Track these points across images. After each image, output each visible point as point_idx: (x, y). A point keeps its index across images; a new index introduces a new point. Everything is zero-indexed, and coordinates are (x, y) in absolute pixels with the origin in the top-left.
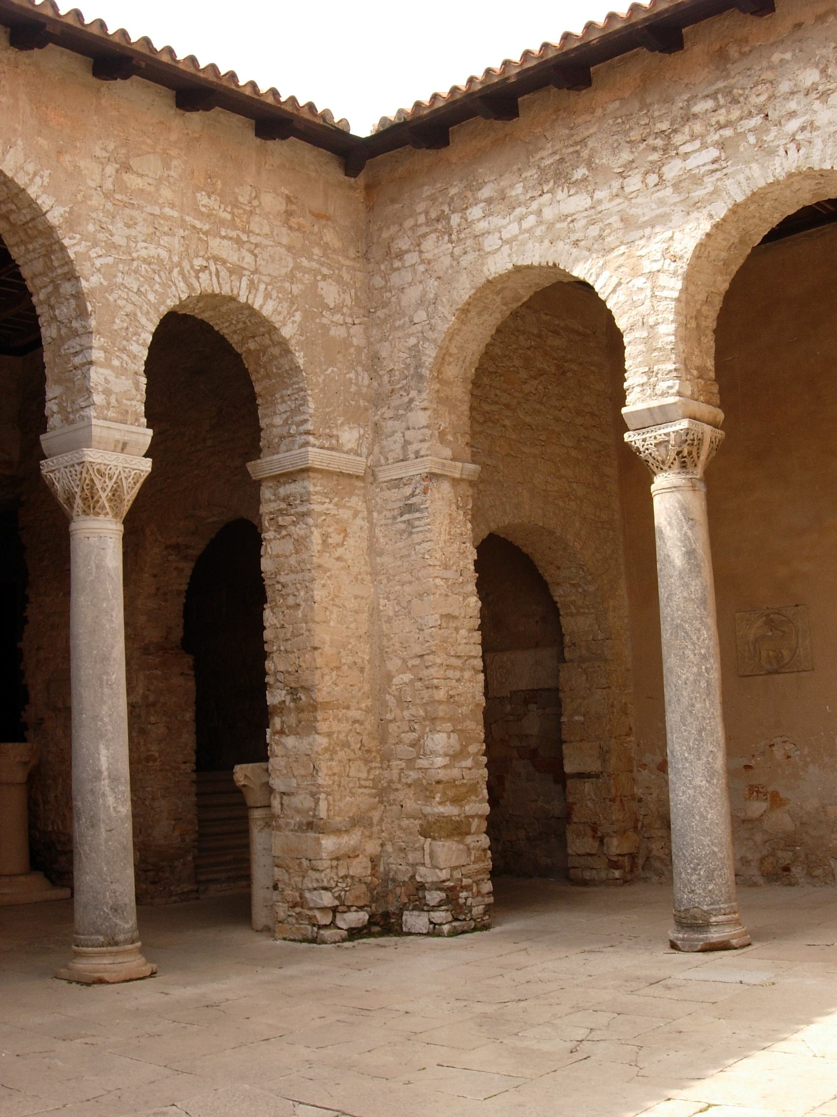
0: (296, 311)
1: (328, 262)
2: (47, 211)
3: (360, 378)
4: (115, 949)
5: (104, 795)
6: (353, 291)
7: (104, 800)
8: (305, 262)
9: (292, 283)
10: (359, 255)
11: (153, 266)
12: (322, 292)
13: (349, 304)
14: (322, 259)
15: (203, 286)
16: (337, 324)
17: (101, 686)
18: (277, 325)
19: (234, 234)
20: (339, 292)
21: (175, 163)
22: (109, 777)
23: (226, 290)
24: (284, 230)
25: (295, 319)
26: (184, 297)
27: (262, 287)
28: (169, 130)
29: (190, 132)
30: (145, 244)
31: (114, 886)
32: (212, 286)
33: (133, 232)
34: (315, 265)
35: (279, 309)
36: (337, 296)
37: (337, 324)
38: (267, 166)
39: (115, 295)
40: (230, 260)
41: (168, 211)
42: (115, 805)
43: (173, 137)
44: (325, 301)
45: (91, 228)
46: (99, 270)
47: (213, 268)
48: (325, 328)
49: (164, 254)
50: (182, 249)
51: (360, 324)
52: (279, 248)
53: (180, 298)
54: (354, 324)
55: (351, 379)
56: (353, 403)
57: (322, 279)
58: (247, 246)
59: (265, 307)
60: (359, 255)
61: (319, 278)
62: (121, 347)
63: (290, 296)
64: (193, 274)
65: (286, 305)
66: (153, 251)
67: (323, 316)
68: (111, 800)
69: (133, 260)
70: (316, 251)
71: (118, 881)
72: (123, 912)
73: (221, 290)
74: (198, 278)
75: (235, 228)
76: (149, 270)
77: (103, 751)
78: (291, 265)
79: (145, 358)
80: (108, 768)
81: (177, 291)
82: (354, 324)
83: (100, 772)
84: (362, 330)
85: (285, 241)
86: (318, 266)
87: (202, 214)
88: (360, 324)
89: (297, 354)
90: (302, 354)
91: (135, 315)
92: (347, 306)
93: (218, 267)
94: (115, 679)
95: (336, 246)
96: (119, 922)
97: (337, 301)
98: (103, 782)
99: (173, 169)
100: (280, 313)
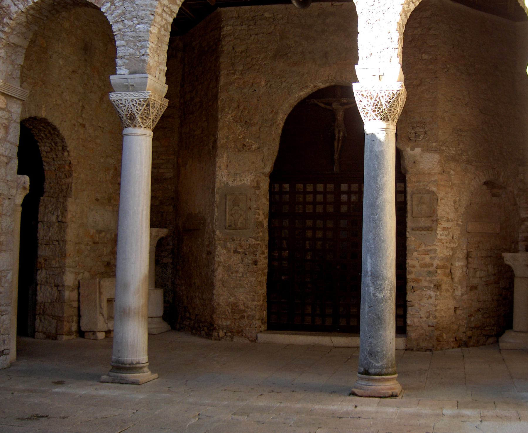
4: (367, 377)
5: (368, 286)
7: (368, 289)
17: (370, 222)
22: (371, 275)
31: (370, 340)
42: (374, 292)
68: (372, 289)
71: (373, 337)
72: (375, 356)
77: (369, 260)
80: (371, 270)
83: (367, 272)
94: (378, 218)
96: (372, 361)
98: (368, 278)
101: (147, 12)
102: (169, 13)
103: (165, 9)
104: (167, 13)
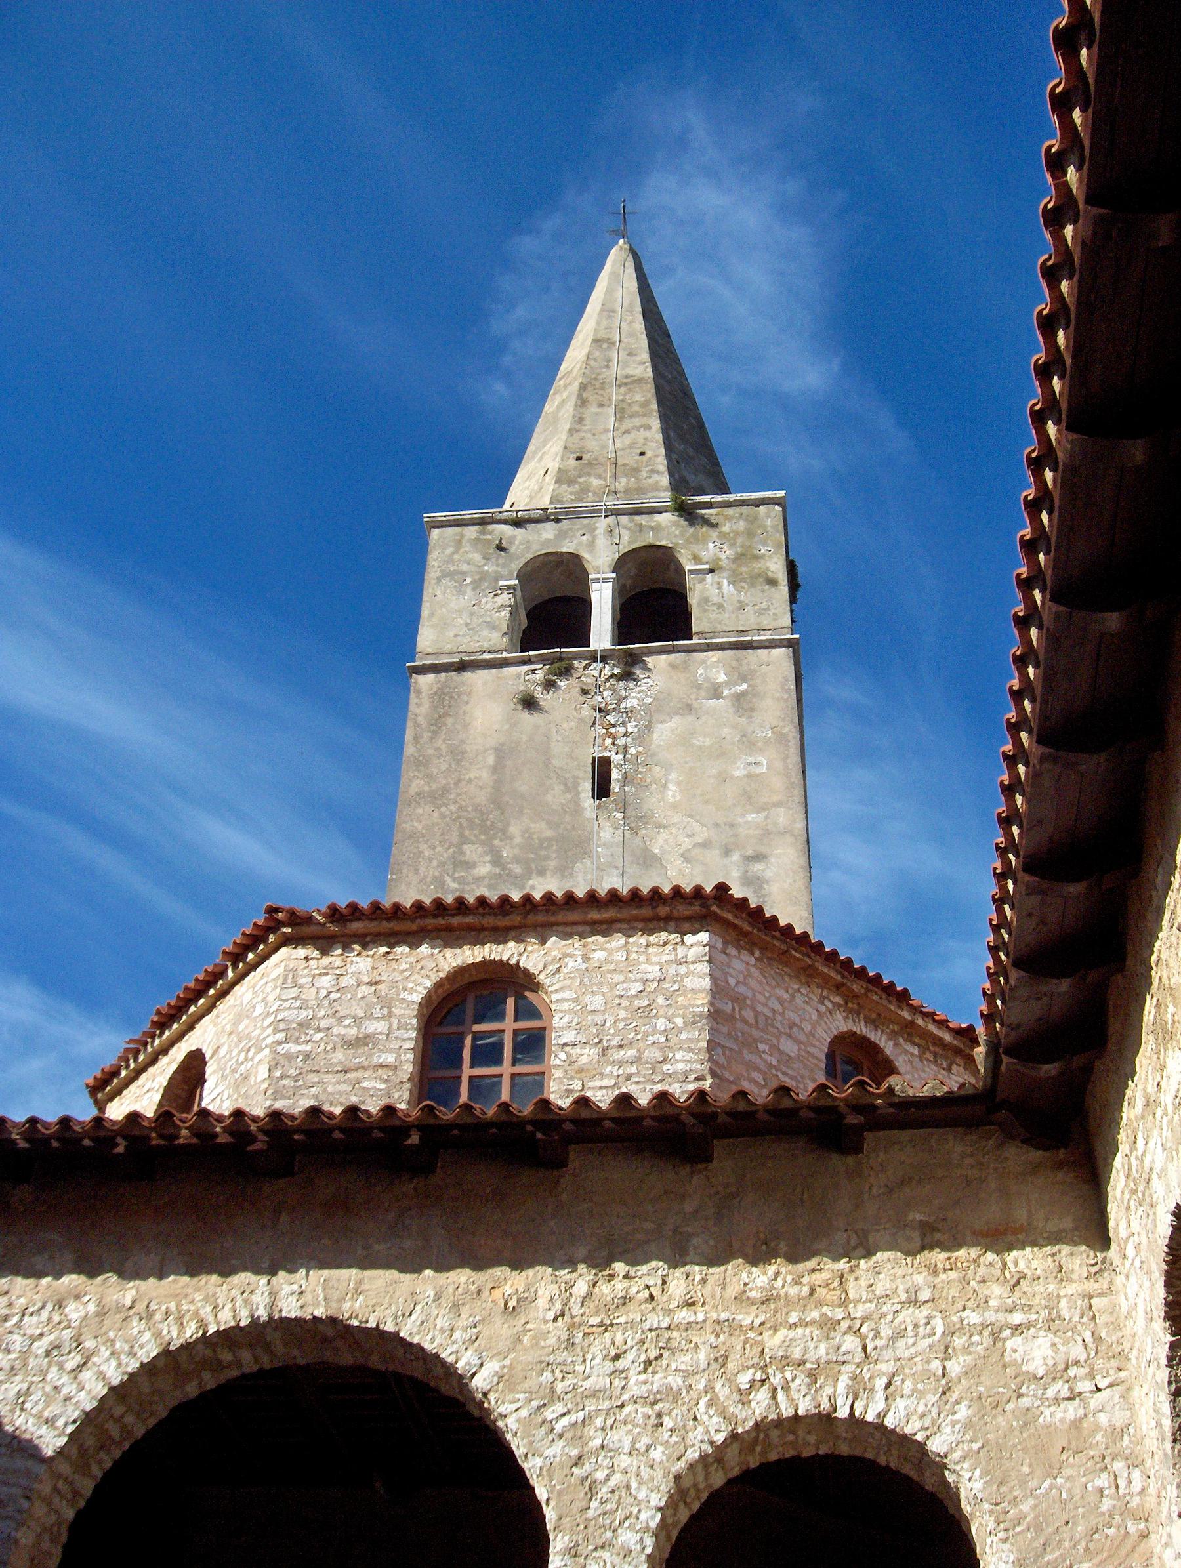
0: (957, 1402)
1: (1023, 1301)
2: (474, 1375)
3: (1122, 1483)
6: (1087, 1335)
8: (973, 1318)
9: (946, 1358)
10: (1096, 1268)
11: (657, 1407)
12: (1017, 1356)
13: (1082, 1358)
14: (1009, 1301)
15: (757, 1412)
16: (1057, 1401)
18: (919, 1437)
19: (815, 1315)
20: (1054, 1345)
21: (695, 1241)
23: (804, 1407)
24: (919, 1279)
25: (957, 1417)
26: (720, 1438)
27: (881, 1383)
28: (683, 1197)
29: (720, 1188)
30: (643, 1377)
32: (777, 1406)
33: (621, 1364)
34: (990, 1316)
35: (921, 1408)
36: (1049, 1352)
37: (1057, 1401)
38: (874, 1191)
39: (587, 1467)
40: (811, 1355)
41: (684, 1315)
43: (688, 1207)
44: (1024, 1368)
45: (547, 1376)
46: (561, 1436)
47: (776, 1380)
48: (1028, 1417)
49: (676, 1381)
50: (714, 1366)
51: (1111, 1385)
52: (911, 1309)
53: (712, 1443)
54: (1099, 1390)
55: (1101, 1490)
56: (1111, 1532)
57: (1013, 1335)
58: (845, 1325)
59: (891, 1414)
60: (1094, 1270)
61: (1006, 1333)
62: (600, 1542)
63: (943, 1382)
64: (735, 1396)
65: (932, 1398)
66: (657, 1381)
67: (1020, 1396)
69: (622, 1406)
70: (997, 1292)
73: (796, 1411)
74: (745, 1403)
75: (820, 1304)
76: (650, 1413)
78: (940, 1330)
79: (649, 1550)
81: (708, 1431)
82: (1099, 1390)
84: (1116, 1399)
85: (925, 1295)
86: (1001, 1317)
87: (753, 1302)
88: (1111, 1385)
89: (967, 1475)
90: (977, 1473)
91: (628, 1487)
92: (1077, 1363)
93: (788, 1375)
95: (1039, 1272)
97: (1051, 1363)
99: (692, 1253)
100: (922, 1416)
101: (14, 1490)
102: (69, 1496)
103: (60, 1484)
104: (63, 1497)
